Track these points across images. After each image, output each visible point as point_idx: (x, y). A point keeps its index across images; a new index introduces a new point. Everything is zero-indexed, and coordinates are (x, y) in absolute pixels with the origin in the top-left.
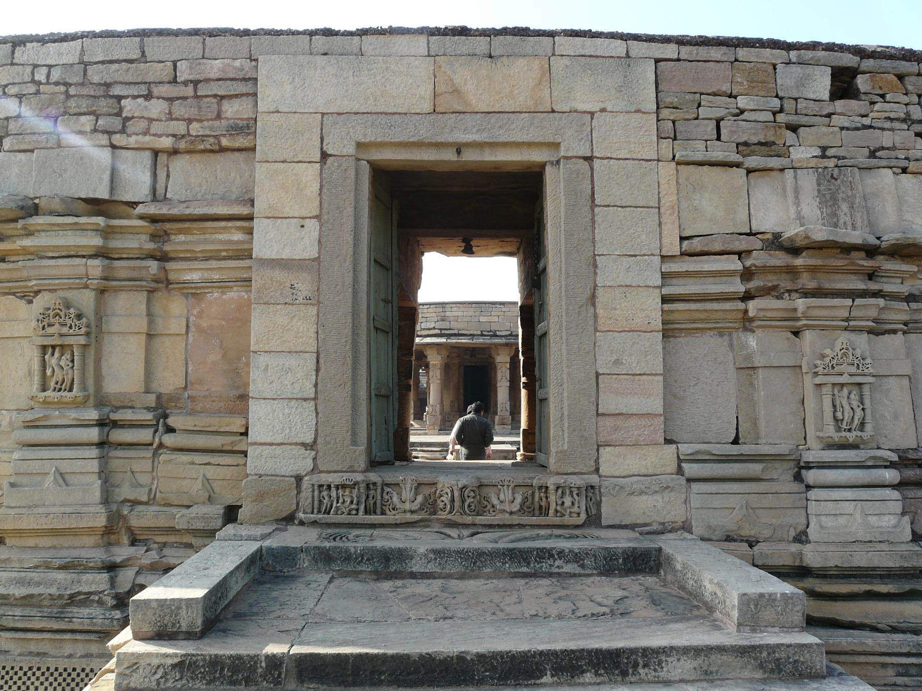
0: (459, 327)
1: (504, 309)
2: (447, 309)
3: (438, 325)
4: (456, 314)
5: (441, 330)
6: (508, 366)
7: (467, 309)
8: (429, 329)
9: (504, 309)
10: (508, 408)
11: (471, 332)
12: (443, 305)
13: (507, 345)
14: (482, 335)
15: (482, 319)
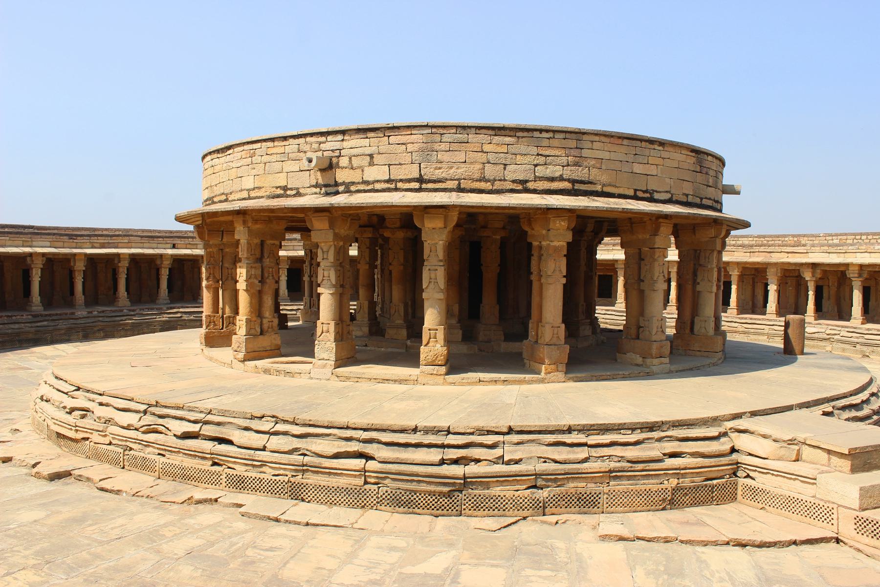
0: (604, 178)
1: (665, 154)
3: (568, 173)
4: (600, 154)
5: (574, 182)
7: (616, 148)
8: (552, 179)
9: (665, 154)
12: (579, 134)
14: (635, 197)
15: (638, 168)
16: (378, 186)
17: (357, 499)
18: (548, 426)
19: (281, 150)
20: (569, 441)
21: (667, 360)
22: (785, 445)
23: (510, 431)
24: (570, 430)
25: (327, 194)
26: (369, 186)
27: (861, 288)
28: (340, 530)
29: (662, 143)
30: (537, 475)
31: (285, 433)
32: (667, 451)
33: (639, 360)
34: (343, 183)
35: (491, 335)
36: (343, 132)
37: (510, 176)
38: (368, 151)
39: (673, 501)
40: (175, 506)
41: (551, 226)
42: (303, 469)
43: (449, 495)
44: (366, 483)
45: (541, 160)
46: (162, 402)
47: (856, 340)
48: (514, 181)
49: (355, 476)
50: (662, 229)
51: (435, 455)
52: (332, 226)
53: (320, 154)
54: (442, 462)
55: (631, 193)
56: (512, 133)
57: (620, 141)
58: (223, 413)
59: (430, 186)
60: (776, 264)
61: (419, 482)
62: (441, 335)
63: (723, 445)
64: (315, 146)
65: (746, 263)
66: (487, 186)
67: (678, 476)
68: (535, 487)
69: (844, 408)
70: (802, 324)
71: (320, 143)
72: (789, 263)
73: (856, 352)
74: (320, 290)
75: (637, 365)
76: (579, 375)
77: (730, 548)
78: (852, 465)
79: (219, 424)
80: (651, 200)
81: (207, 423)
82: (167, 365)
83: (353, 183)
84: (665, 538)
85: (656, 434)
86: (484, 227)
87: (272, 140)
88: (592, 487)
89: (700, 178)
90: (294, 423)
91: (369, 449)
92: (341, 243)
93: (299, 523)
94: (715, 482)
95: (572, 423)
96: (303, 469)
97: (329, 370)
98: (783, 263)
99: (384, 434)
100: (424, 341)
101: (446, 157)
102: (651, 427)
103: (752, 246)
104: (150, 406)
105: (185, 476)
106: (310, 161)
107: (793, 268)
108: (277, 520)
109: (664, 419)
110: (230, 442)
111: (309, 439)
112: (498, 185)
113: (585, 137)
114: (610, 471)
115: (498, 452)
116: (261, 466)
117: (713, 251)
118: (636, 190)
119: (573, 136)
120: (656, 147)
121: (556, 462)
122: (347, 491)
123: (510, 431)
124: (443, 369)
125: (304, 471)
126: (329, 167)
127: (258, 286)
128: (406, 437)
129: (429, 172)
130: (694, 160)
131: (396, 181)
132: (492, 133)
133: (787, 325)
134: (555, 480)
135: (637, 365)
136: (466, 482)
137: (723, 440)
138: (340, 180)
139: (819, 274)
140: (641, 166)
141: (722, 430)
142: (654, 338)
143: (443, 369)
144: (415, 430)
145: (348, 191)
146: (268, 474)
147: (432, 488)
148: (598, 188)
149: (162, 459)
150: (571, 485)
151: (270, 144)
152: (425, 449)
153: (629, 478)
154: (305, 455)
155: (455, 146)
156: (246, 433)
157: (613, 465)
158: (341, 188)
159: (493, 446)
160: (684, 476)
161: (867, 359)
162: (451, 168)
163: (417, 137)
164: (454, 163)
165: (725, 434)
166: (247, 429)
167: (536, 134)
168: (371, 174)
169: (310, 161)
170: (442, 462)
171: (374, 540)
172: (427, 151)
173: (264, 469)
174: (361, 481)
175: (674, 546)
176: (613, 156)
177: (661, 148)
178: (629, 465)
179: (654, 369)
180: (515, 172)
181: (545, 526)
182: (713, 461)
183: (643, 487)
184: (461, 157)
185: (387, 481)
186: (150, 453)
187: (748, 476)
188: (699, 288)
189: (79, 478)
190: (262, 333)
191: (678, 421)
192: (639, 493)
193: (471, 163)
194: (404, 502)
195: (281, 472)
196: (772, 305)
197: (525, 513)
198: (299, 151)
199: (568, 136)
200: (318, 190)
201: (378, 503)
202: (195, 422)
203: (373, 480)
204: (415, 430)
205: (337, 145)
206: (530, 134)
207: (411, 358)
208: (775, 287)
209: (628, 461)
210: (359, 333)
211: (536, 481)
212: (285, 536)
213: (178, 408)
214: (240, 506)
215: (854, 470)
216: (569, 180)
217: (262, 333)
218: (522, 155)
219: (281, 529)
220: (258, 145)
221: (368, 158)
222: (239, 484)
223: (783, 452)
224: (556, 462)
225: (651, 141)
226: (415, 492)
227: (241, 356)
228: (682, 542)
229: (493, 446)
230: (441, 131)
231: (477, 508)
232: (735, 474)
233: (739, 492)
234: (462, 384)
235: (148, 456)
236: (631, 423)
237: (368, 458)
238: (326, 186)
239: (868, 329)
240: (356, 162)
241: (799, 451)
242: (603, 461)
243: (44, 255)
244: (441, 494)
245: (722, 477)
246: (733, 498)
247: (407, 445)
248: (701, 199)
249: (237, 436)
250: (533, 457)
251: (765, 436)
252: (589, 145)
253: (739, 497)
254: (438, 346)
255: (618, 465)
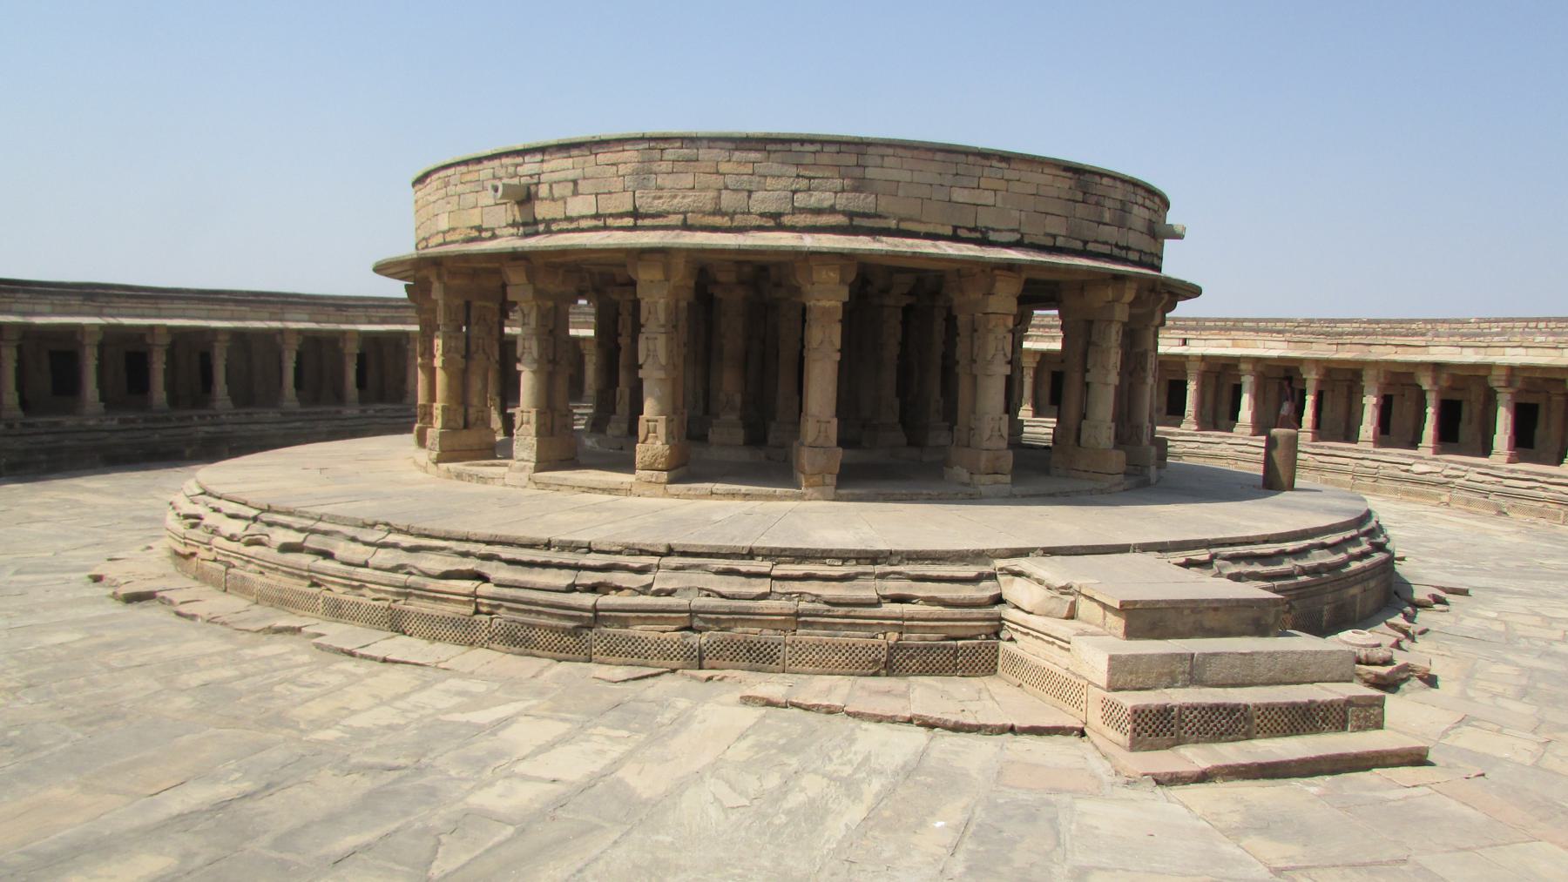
1: (1009, 174)
2: (870, 160)
3: (842, 201)
4: (895, 175)
5: (851, 215)
6: (1010, 323)
9: (1009, 174)
10: (1006, 435)
11: (930, 229)
12: (860, 146)
13: (1010, 267)
14: (955, 238)
15: (959, 195)
16: (584, 224)
17: (464, 632)
18: (720, 547)
19: (474, 177)
20: (743, 569)
21: (1008, 478)
22: (1056, 594)
23: (670, 552)
24: (751, 554)
25: (526, 235)
26: (572, 223)
27: (1511, 405)
28: (419, 670)
29: (1006, 158)
30: (693, 613)
31: (395, 546)
32: (887, 593)
33: (965, 476)
34: (544, 220)
35: (737, 433)
36: (542, 150)
37: (756, 207)
38: (571, 175)
39: (890, 664)
40: (247, 635)
41: (815, 277)
42: (406, 592)
43: (575, 632)
44: (477, 612)
45: (803, 183)
46: (274, 506)
47: (1489, 487)
48: (762, 215)
49: (464, 603)
50: (998, 284)
51: (563, 579)
52: (531, 278)
53: (515, 181)
54: (572, 588)
55: (948, 231)
56: (760, 146)
57: (930, 155)
58: (334, 519)
59: (648, 222)
60: (1376, 363)
61: (539, 613)
62: (662, 429)
63: (986, 590)
64: (511, 170)
65: (1328, 361)
66: (725, 221)
67: (901, 630)
68: (690, 628)
69: (1235, 559)
70: (1293, 441)
71: (517, 165)
72: (1394, 363)
73: (1487, 506)
74: (519, 367)
75: (964, 484)
76: (857, 491)
77: (913, 728)
78: (1127, 627)
79: (326, 533)
80: (984, 242)
81: (313, 532)
82: (379, 477)
83: (554, 220)
84: (828, 707)
85: (878, 569)
86: (778, 285)
87: (466, 163)
88: (769, 634)
89: (1080, 210)
90: (407, 533)
91: (487, 568)
92: (550, 304)
93: (374, 659)
94: (960, 643)
95: (757, 544)
96: (406, 592)
97: (524, 476)
98: (1388, 363)
99: (509, 549)
100: (641, 438)
101: (667, 181)
102: (874, 557)
103: (1341, 334)
104: (263, 511)
105: (283, 602)
106: (496, 190)
107: (1404, 370)
108: (351, 654)
109: (894, 548)
110: (328, 555)
111: (420, 554)
112: (739, 220)
113: (871, 150)
114: (797, 614)
115: (646, 579)
116: (360, 587)
117: (1111, 321)
118: (955, 228)
119: (852, 148)
120: (995, 163)
121: (722, 596)
122: (454, 622)
123: (670, 552)
124: (664, 476)
125: (407, 595)
126: (526, 198)
127: (461, 363)
128: (538, 552)
129: (646, 203)
130: (1066, 184)
131: (605, 216)
132: (730, 146)
133: (1271, 444)
134: (717, 621)
135: (964, 484)
136: (597, 617)
137: (983, 584)
138: (539, 217)
139: (1444, 381)
140: (966, 192)
141: (987, 569)
142: (986, 445)
143: (664, 476)
144: (548, 545)
145: (549, 232)
146: (367, 598)
147: (554, 622)
148: (892, 224)
149: (261, 579)
150: (740, 629)
151: (463, 169)
152: (555, 571)
153: (826, 626)
154: (410, 573)
155: (680, 166)
156: (353, 545)
157: (803, 605)
158: (541, 227)
159: (643, 570)
160: (910, 629)
161: (1502, 518)
162: (675, 197)
163: (631, 154)
164: (679, 189)
165: (992, 577)
166: (354, 539)
167: (796, 147)
168: (580, 206)
169: (496, 190)
170: (572, 588)
171: (454, 683)
172: (643, 174)
173: (364, 591)
174: (470, 610)
175: (836, 720)
176: (917, 177)
177: (1003, 165)
178: (827, 607)
179: (982, 489)
180: (766, 200)
181: (694, 682)
182: (957, 612)
183: (844, 641)
184: (688, 180)
185: (501, 611)
186: (251, 573)
187: (1011, 639)
188: (1089, 378)
189: (163, 601)
190: (466, 426)
191: (916, 552)
192: (837, 649)
193: (702, 190)
194: (519, 640)
195: (382, 595)
196: (1246, 413)
197: (675, 664)
198: (494, 177)
199: (844, 148)
200: (514, 231)
201: (490, 641)
202: (301, 530)
203: (485, 609)
204: (548, 545)
205: (534, 168)
206: (787, 147)
207: (625, 463)
208: (1374, 400)
209: (826, 603)
210: (617, 432)
211: (691, 621)
212: (342, 672)
213: (289, 513)
214: (321, 635)
215: (1131, 633)
216: (844, 213)
217: (466, 426)
218: (773, 176)
219: (349, 665)
220: (451, 171)
221: (571, 185)
222: (336, 611)
223: (1053, 604)
224: (722, 596)
225: (985, 155)
226: (533, 626)
227: (434, 455)
228: (849, 714)
229: (643, 570)
230: (662, 145)
231: (610, 652)
232: (997, 635)
233: (1000, 662)
234: (687, 497)
235: (248, 575)
236: (840, 551)
237: (484, 578)
238: (525, 224)
239: (1512, 471)
240: (557, 191)
241: (1073, 604)
242: (790, 600)
243: (299, 332)
244: (565, 631)
245: (971, 638)
246: (990, 669)
247: (531, 564)
248: (1085, 243)
249: (342, 549)
250: (695, 588)
251: (1040, 582)
252: (879, 161)
253: (1000, 669)
254: (659, 443)
255: (811, 606)
